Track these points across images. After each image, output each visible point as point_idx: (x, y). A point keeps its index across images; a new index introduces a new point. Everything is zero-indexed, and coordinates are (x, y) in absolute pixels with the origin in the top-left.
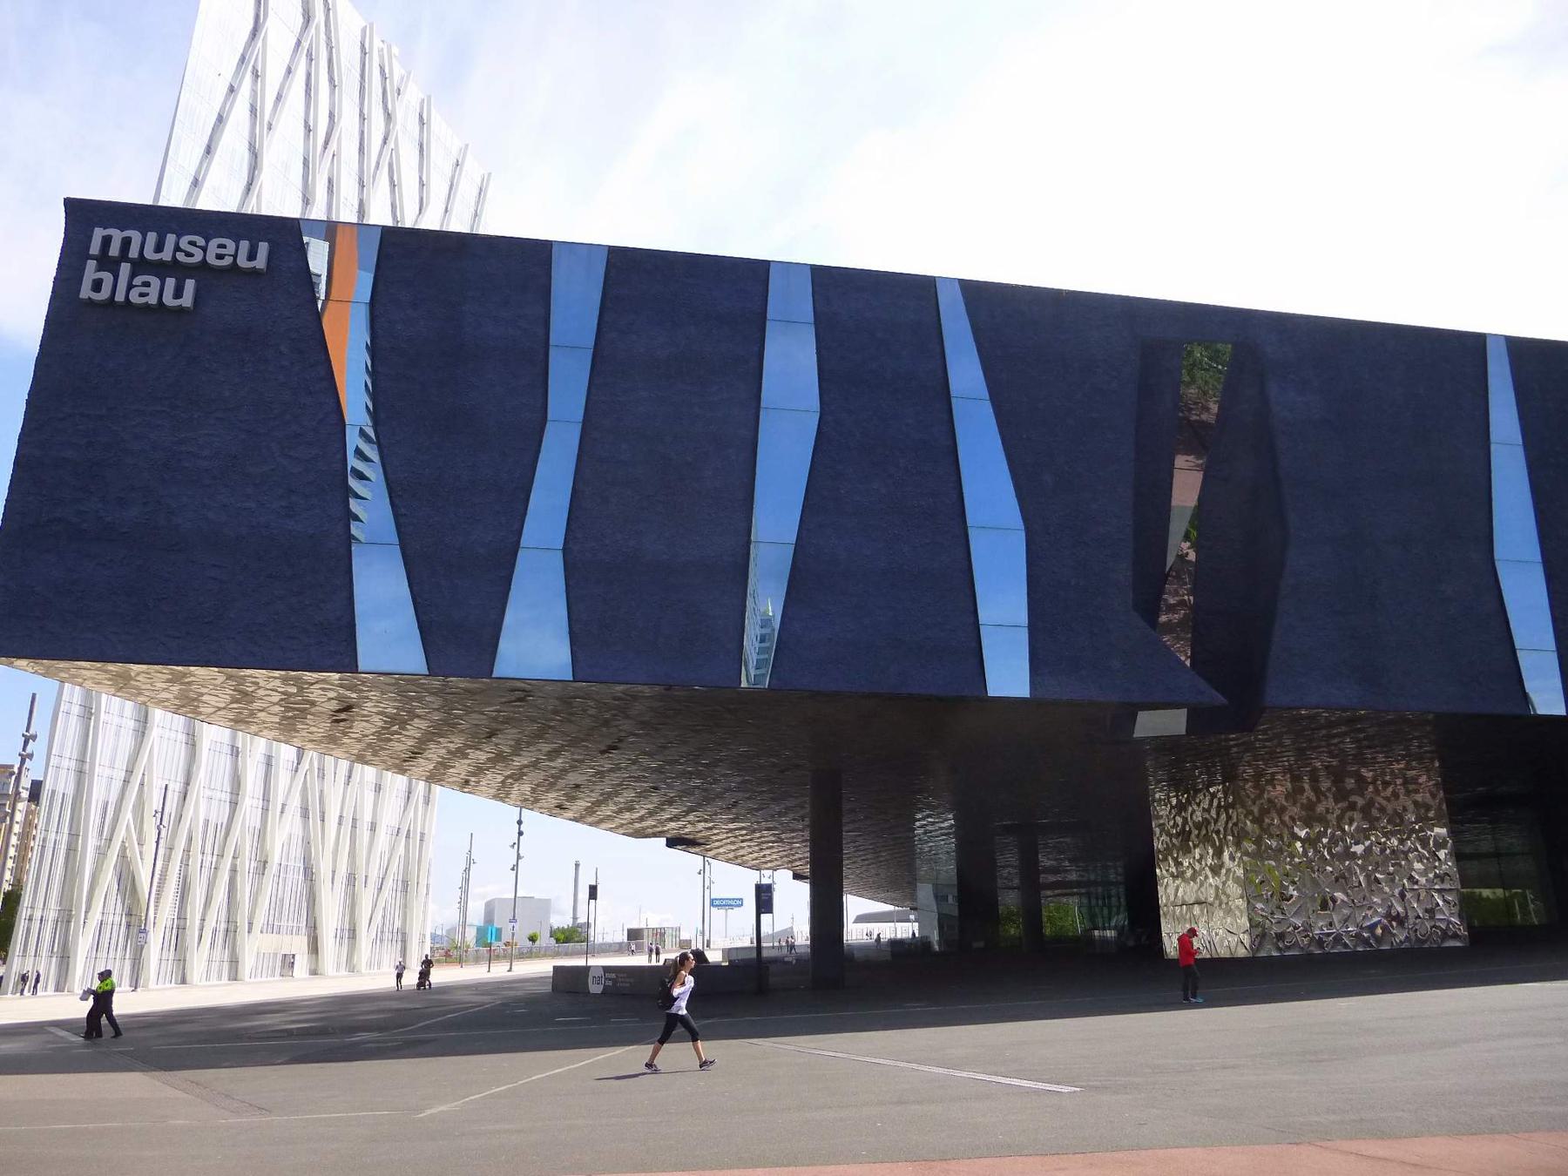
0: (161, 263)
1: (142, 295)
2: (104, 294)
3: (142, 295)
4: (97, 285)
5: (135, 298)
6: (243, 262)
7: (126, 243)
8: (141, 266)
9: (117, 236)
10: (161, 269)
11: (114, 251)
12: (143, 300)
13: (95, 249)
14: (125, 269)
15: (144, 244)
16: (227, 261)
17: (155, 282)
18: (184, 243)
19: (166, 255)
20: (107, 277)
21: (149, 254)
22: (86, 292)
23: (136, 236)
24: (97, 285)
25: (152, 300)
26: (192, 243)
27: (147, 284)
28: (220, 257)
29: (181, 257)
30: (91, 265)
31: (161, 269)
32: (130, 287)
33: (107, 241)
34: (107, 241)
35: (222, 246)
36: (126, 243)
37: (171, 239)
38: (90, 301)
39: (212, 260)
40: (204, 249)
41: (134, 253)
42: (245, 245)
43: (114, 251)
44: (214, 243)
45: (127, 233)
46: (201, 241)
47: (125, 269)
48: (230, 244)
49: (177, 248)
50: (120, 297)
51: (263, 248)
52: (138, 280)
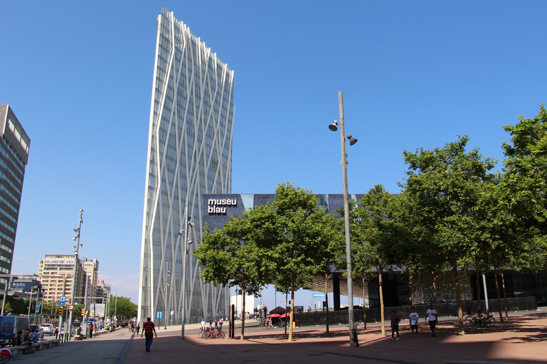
0: (220, 205)
1: (218, 211)
2: (212, 212)
3: (218, 211)
4: (210, 210)
5: (217, 212)
6: (233, 204)
7: (214, 202)
8: (217, 206)
9: (212, 201)
10: (220, 206)
11: (212, 203)
12: (218, 212)
13: (209, 204)
14: (214, 206)
15: (217, 201)
16: (230, 204)
17: (219, 208)
18: (223, 201)
19: (220, 204)
20: (212, 208)
21: (218, 204)
22: (209, 211)
23: (215, 200)
24: (210, 210)
25: (219, 212)
26: (224, 201)
27: (218, 209)
28: (229, 203)
29: (223, 203)
30: (209, 206)
31: (220, 206)
32: (216, 210)
33: (211, 202)
34: (211, 202)
35: (229, 201)
36: (214, 202)
37: (221, 200)
38: (210, 213)
39: (228, 204)
40: (226, 202)
41: (215, 204)
42: (232, 200)
43: (212, 203)
44: (228, 200)
45: (214, 200)
46: (225, 200)
47: (214, 206)
48: (230, 200)
49: (222, 202)
50: (214, 212)
51: (235, 200)
52: (217, 208)
